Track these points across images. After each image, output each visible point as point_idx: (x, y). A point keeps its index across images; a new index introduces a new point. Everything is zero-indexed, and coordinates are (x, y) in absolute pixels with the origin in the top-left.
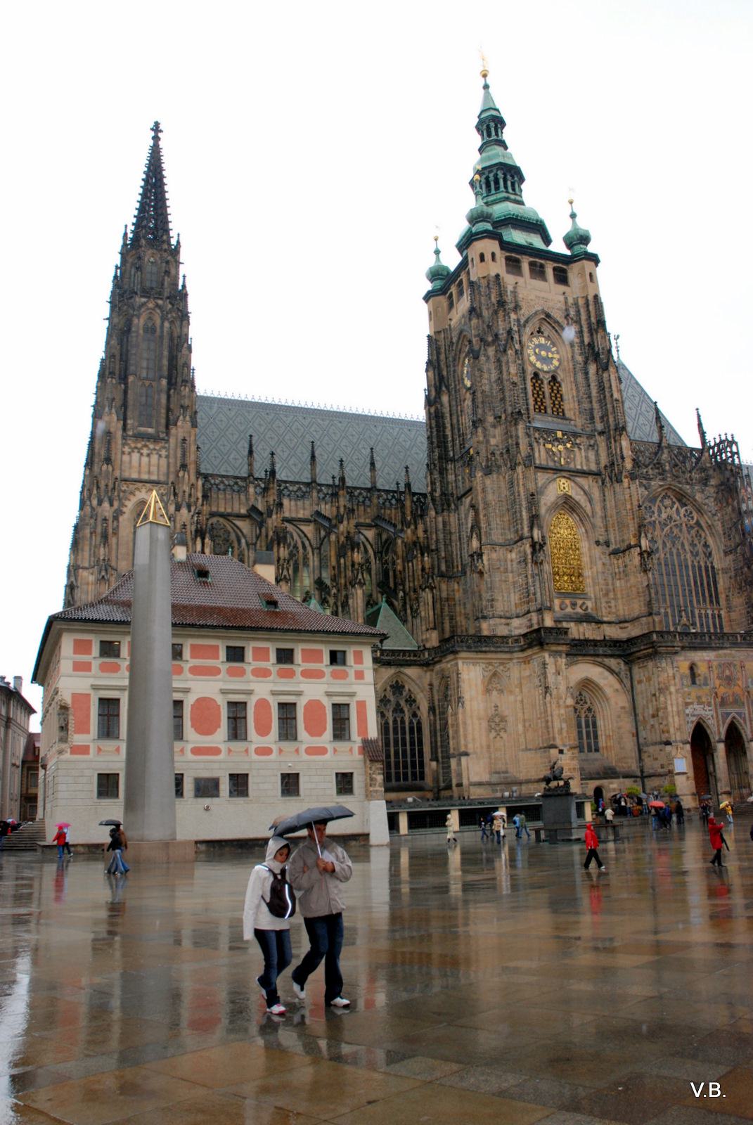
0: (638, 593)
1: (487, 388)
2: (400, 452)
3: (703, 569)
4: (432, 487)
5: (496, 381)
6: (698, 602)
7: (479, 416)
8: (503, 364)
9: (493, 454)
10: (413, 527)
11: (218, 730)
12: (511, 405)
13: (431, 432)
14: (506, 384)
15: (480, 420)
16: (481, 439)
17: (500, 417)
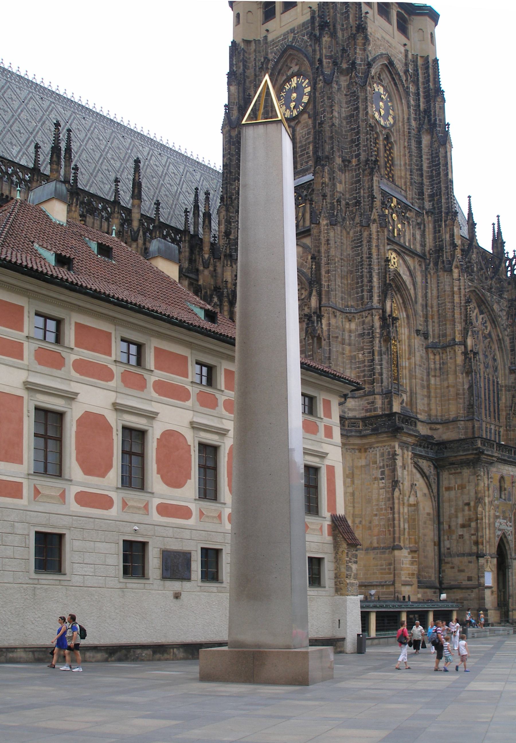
0: (457, 394)
1: (337, 122)
2: (153, 177)
3: (491, 382)
4: (226, 225)
5: (346, 118)
6: (486, 415)
7: (327, 154)
8: (360, 100)
9: (339, 201)
10: (211, 268)
11: (189, 481)
12: (365, 151)
13: (230, 160)
14: (363, 125)
15: (327, 157)
16: (327, 180)
17: (350, 162)
